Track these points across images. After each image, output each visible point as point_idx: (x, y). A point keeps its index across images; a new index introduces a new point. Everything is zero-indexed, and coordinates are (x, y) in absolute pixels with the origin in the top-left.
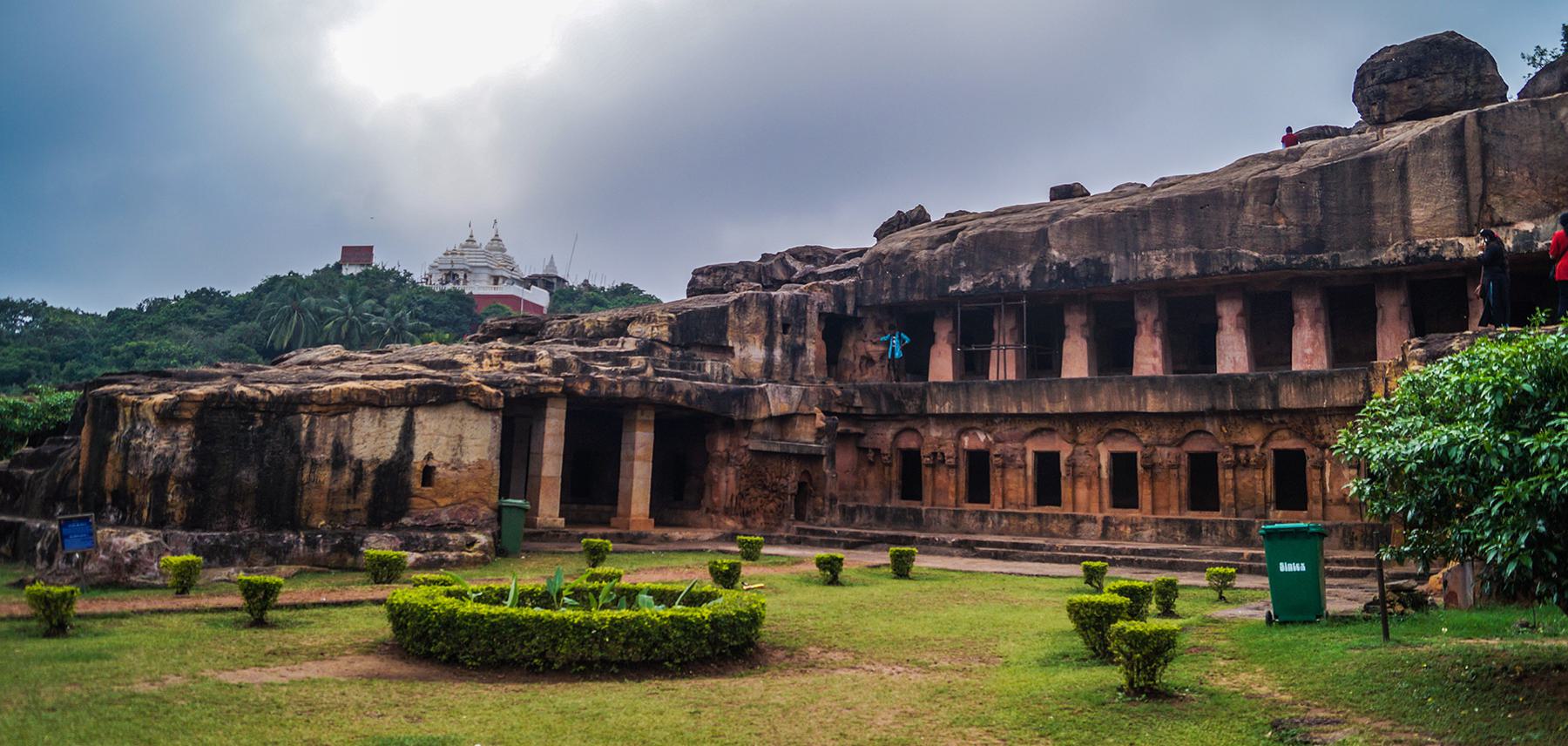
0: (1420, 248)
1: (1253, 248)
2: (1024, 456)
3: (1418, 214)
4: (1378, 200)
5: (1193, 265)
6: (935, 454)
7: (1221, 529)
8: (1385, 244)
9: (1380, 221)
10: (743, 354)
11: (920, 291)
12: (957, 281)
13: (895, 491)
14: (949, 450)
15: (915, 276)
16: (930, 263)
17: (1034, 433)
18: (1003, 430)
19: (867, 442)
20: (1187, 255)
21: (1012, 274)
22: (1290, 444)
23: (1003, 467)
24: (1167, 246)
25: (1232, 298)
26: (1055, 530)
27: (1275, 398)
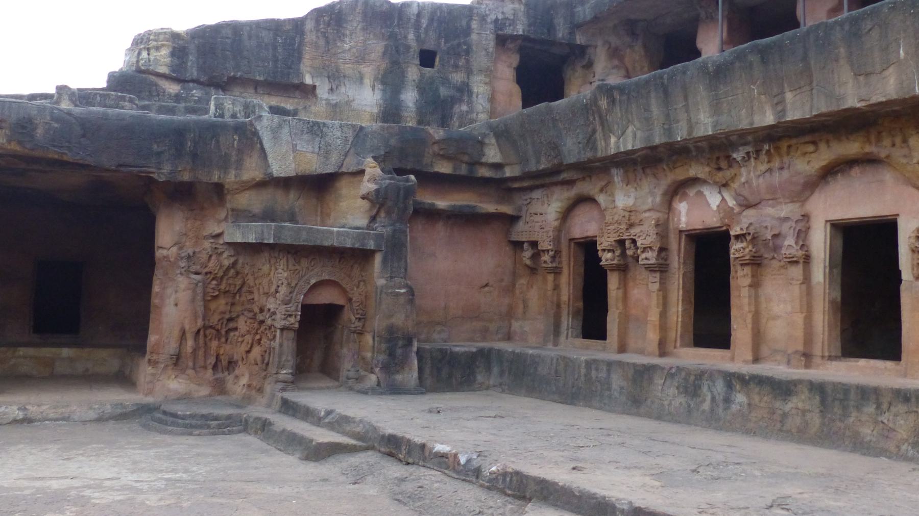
2: (803, 235)
6: (621, 243)
10: (334, 98)
13: (566, 321)
14: (646, 235)
17: (830, 172)
18: (753, 175)
19: (521, 232)
23: (756, 263)
26: (867, 431)
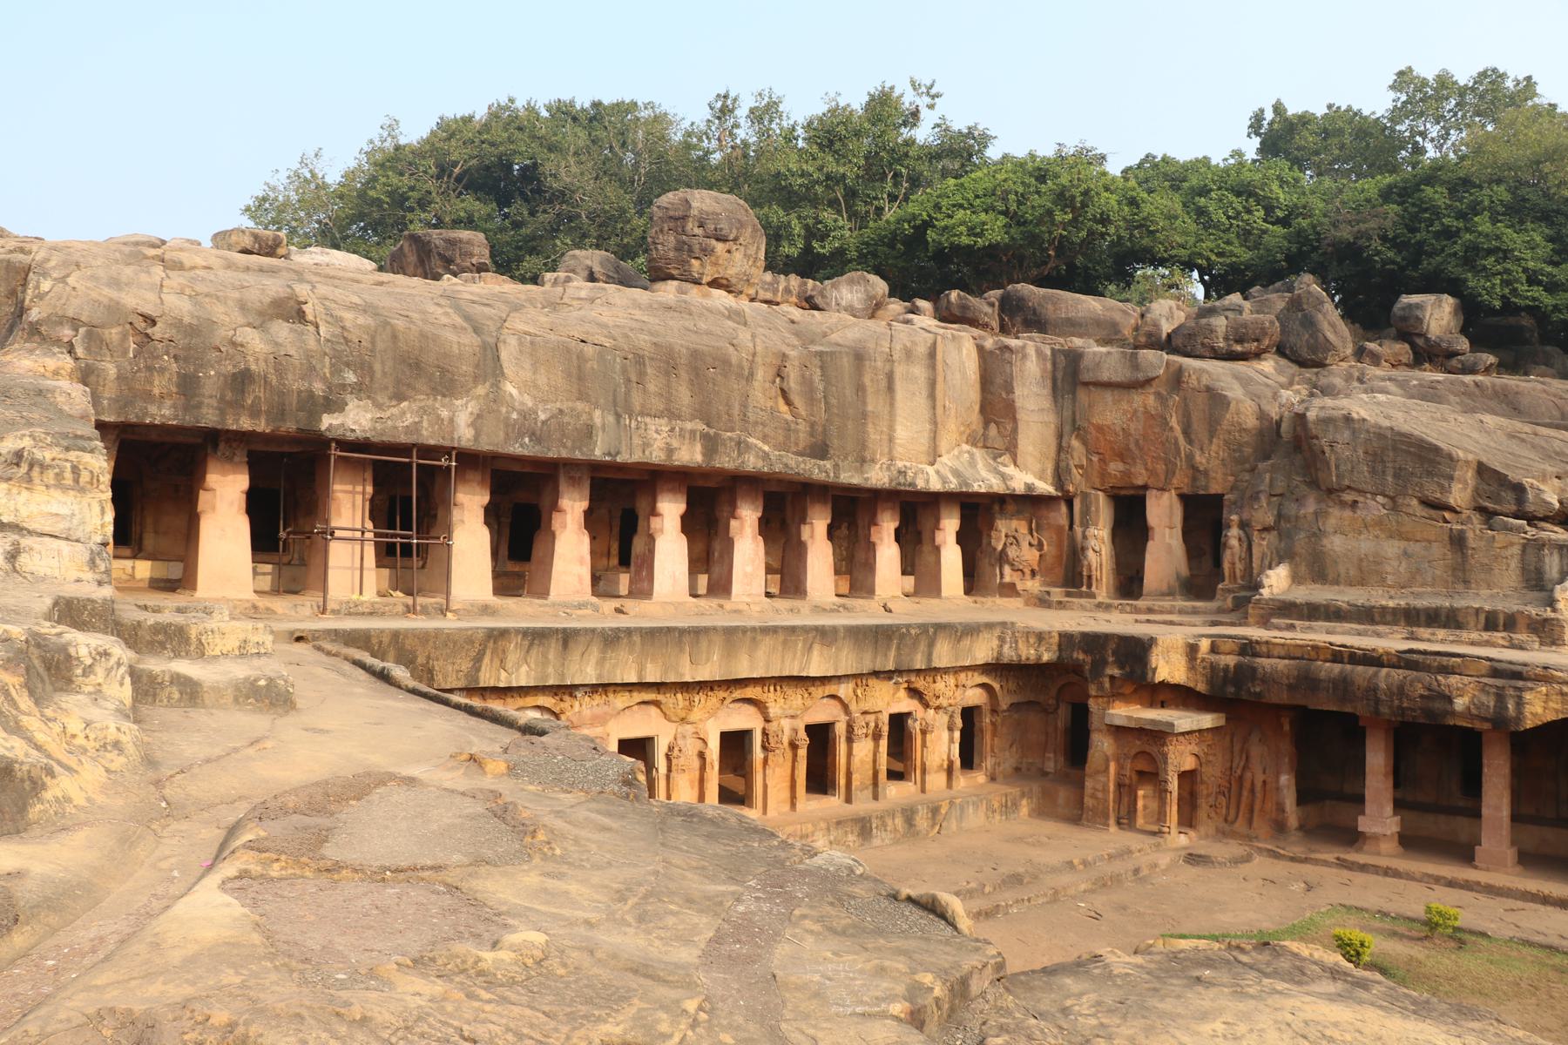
0: (900, 472)
1: (765, 439)
3: (901, 433)
4: (870, 408)
5: (698, 448)
7: (890, 822)
8: (873, 461)
9: (873, 435)
11: (254, 413)
12: (333, 404)
15: (242, 380)
16: (279, 362)
20: (693, 432)
21: (445, 413)
22: (904, 704)
24: (671, 414)
25: (672, 490)
27: (929, 659)
